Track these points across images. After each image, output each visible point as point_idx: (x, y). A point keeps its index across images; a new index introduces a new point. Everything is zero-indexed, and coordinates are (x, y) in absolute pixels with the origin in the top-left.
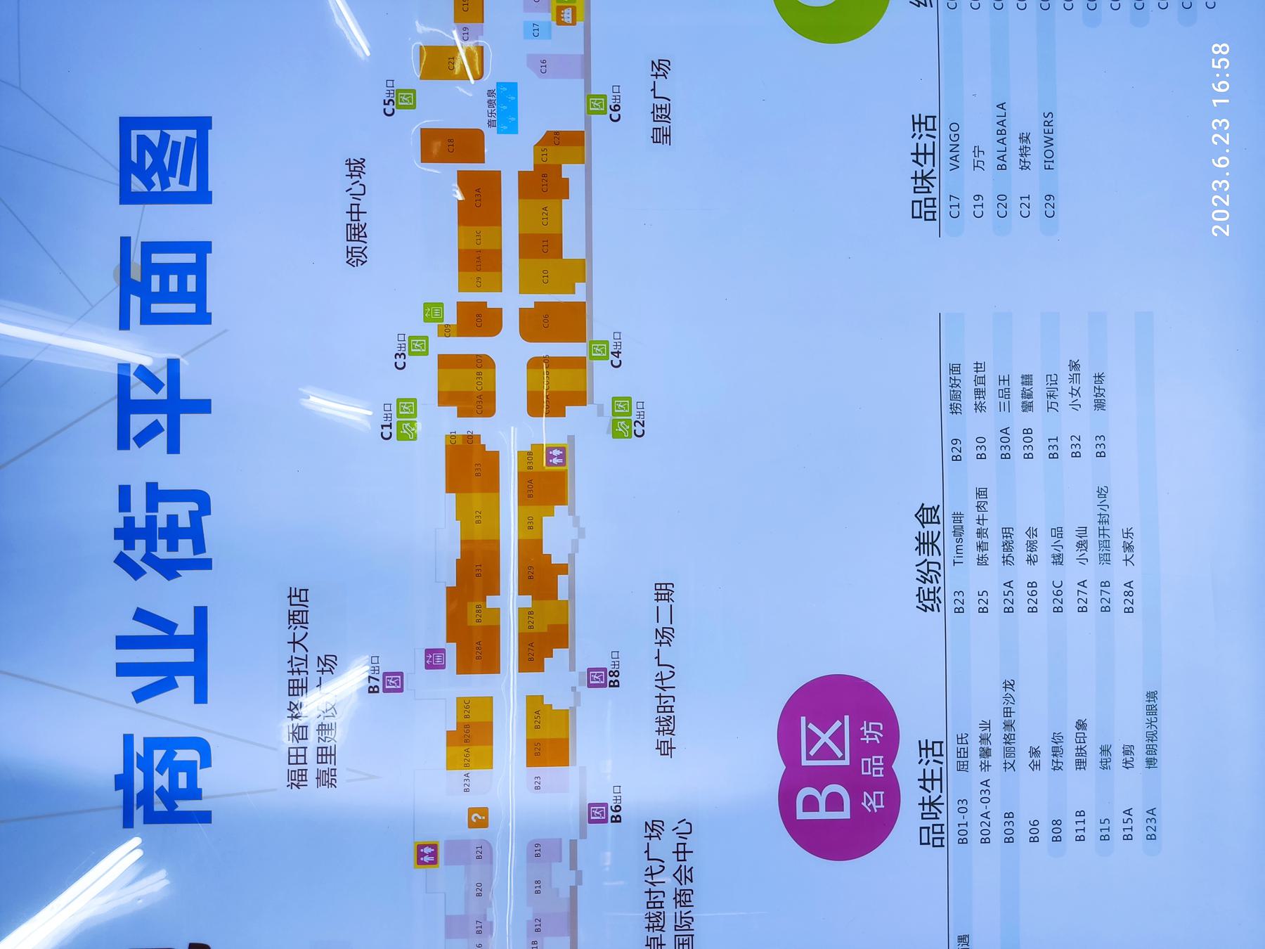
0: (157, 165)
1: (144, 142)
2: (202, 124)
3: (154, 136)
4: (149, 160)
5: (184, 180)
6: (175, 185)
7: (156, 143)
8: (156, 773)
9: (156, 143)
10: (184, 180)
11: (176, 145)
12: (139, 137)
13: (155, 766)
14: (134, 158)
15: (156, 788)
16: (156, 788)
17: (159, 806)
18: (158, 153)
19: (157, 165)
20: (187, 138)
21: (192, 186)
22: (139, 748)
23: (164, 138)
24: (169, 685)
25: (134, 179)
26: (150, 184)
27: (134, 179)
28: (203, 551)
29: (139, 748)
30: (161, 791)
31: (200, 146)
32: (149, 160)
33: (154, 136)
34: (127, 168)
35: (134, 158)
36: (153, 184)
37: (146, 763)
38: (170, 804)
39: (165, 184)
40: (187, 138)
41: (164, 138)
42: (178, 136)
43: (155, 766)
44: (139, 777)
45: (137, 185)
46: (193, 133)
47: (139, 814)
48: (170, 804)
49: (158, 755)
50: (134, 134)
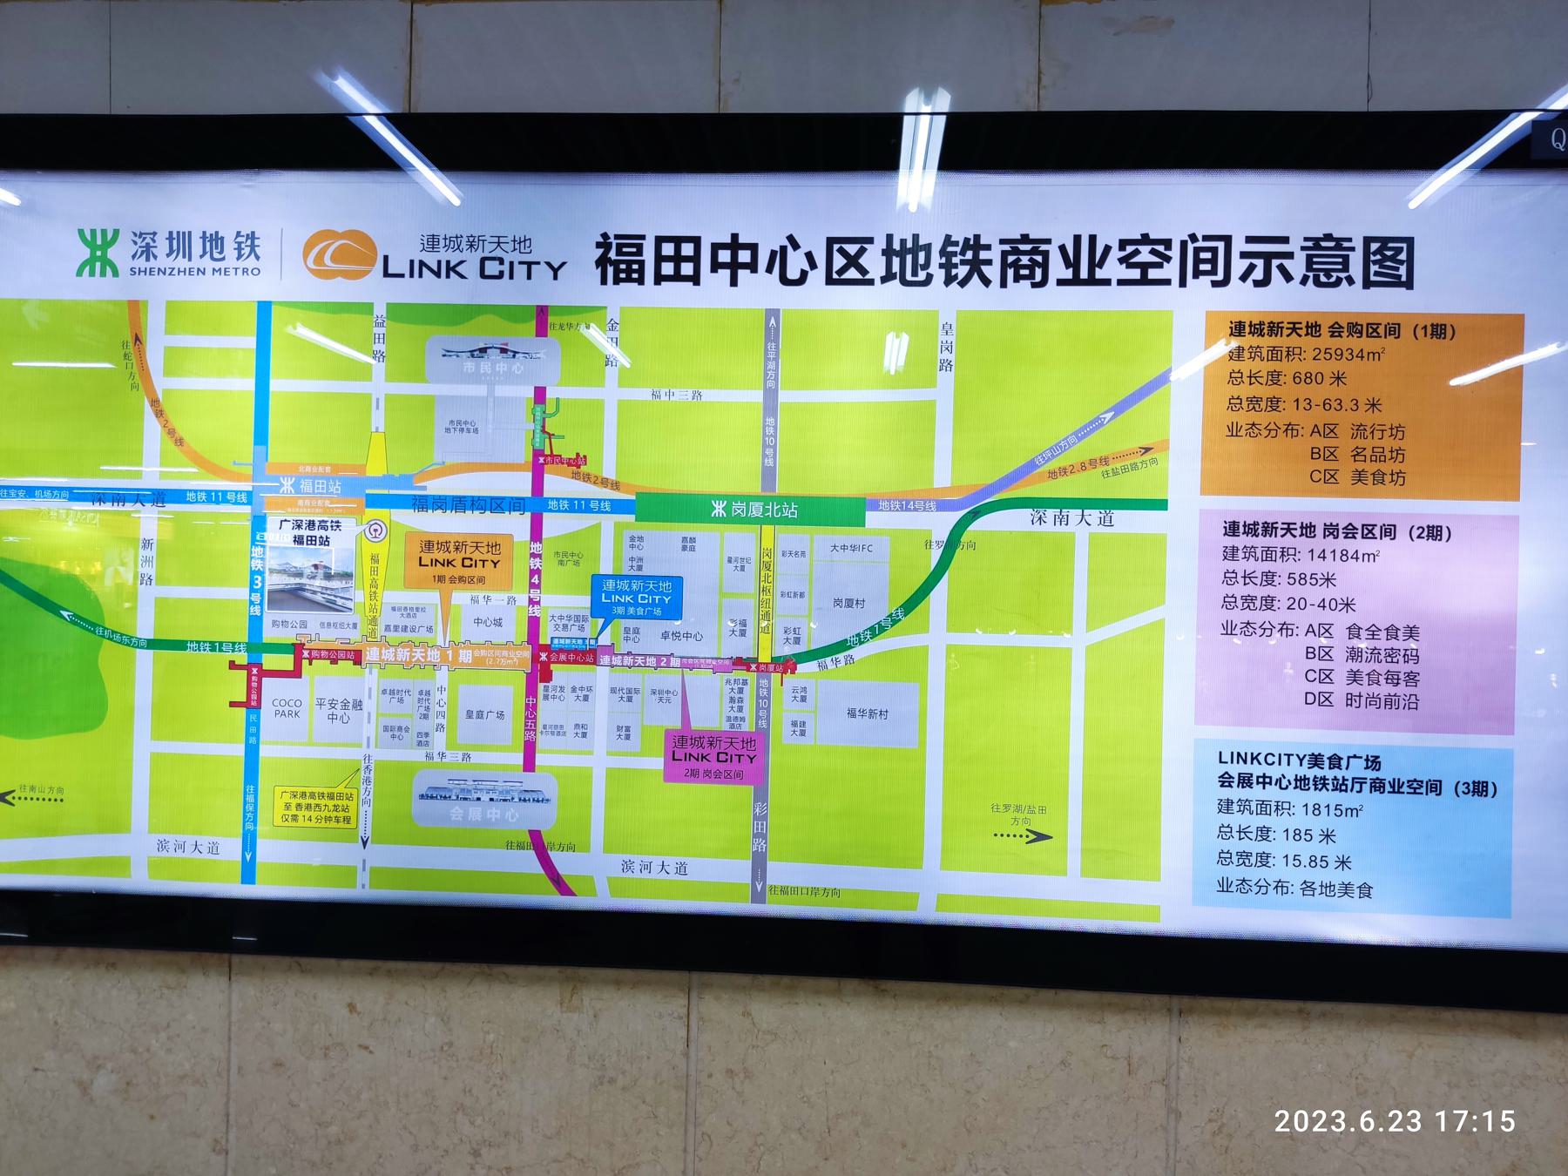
0: (1386, 258)
1: (1400, 250)
2: (1409, 284)
3: (1403, 256)
4: (1389, 253)
5: (1376, 273)
6: (1374, 268)
7: (1399, 258)
8: (1029, 257)
9: (1399, 258)
10: (1376, 273)
11: (1397, 269)
12: (1402, 248)
13: (1034, 257)
14: (1390, 245)
15: (1021, 257)
16: (1021, 257)
17: (1011, 259)
18: (1393, 259)
19: (1386, 258)
20: (1401, 276)
21: (1373, 278)
22: (1043, 247)
23: (1401, 262)
24: (1068, 264)
25: (1378, 245)
26: (1375, 254)
27: (1378, 245)
28: (922, 270)
29: (1043, 247)
30: (1019, 260)
31: (1396, 283)
32: (1389, 253)
33: (1403, 256)
34: (1384, 241)
35: (1390, 245)
36: (1374, 256)
37: (1035, 251)
38: (1011, 265)
39: (1375, 262)
40: (1401, 276)
41: (1401, 262)
42: (1403, 270)
43: (1034, 257)
44: (1028, 247)
45: (1374, 246)
46: (1404, 279)
47: (1007, 247)
48: (1011, 265)
49: (1039, 258)
50: (1404, 245)
